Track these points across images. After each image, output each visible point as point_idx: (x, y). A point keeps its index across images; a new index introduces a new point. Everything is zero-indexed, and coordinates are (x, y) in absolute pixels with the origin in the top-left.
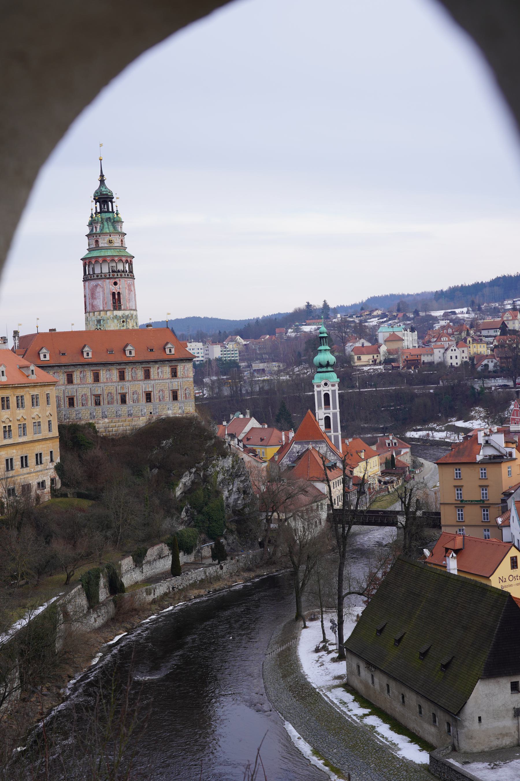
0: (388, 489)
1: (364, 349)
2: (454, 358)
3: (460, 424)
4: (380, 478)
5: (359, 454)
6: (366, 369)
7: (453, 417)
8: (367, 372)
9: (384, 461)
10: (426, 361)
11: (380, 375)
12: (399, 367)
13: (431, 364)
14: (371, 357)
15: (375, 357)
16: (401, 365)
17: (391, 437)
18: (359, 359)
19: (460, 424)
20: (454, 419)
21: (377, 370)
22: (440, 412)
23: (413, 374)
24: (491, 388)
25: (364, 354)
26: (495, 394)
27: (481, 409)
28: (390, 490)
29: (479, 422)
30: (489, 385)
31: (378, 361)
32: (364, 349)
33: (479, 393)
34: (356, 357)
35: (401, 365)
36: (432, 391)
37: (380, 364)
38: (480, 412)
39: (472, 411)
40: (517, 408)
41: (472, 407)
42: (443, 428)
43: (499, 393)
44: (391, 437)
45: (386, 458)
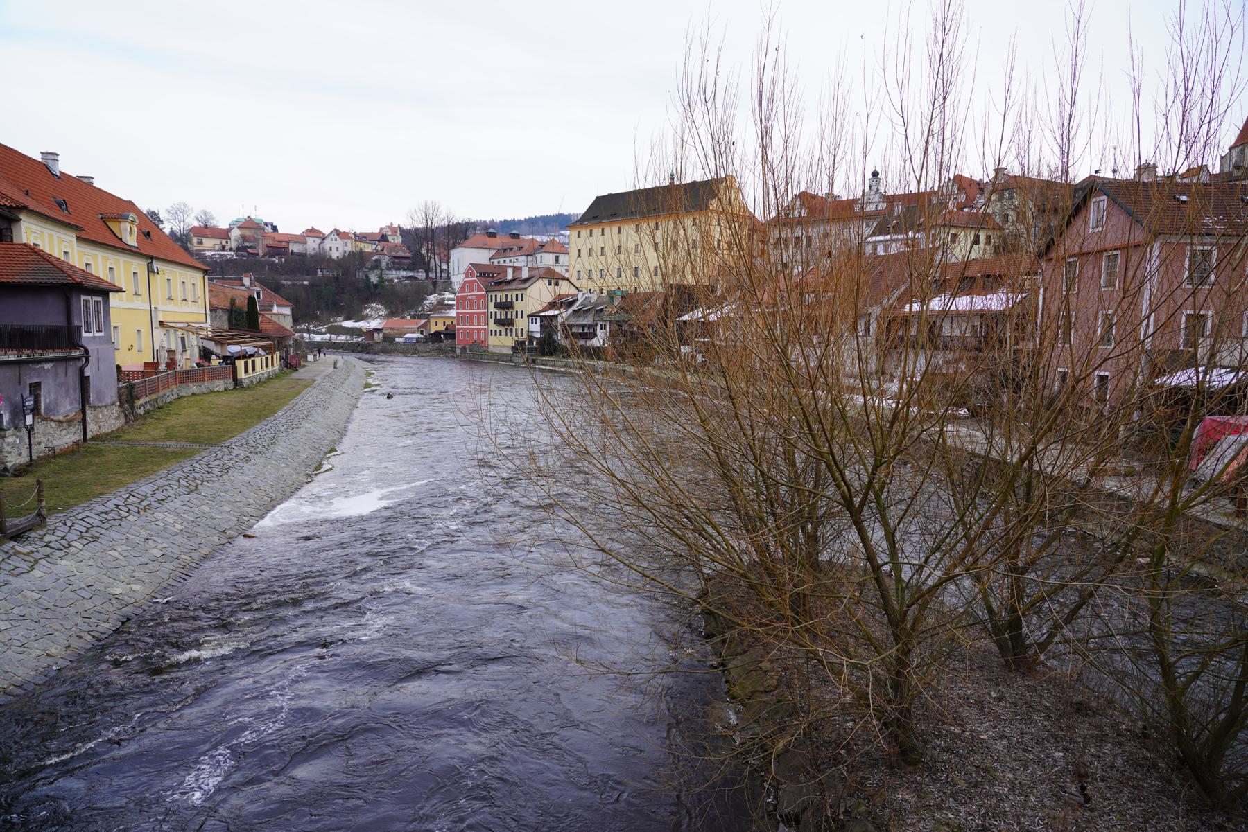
0: (235, 370)
1: (207, 231)
2: (334, 249)
3: (349, 324)
4: (210, 345)
5: (113, 226)
6: (208, 253)
7: (338, 315)
8: (211, 257)
9: (227, 305)
10: (295, 251)
11: (230, 261)
12: (257, 254)
13: (303, 255)
14: (218, 241)
15: (224, 242)
16: (261, 253)
17: (246, 281)
18: (200, 243)
19: (349, 324)
20: (340, 318)
21: (225, 255)
22: (318, 309)
23: (277, 264)
24: (392, 280)
25: (207, 237)
26: (399, 288)
27: (380, 306)
28: (241, 374)
29: (378, 321)
30: (390, 277)
31: (227, 248)
32: (207, 231)
33: (376, 286)
34: (195, 240)
35: (261, 253)
36: (306, 283)
37: (231, 250)
38: (378, 310)
39: (365, 308)
40: (473, 276)
41: (367, 302)
42: (324, 330)
43: (405, 286)
44: (246, 281)
45: (233, 302)
